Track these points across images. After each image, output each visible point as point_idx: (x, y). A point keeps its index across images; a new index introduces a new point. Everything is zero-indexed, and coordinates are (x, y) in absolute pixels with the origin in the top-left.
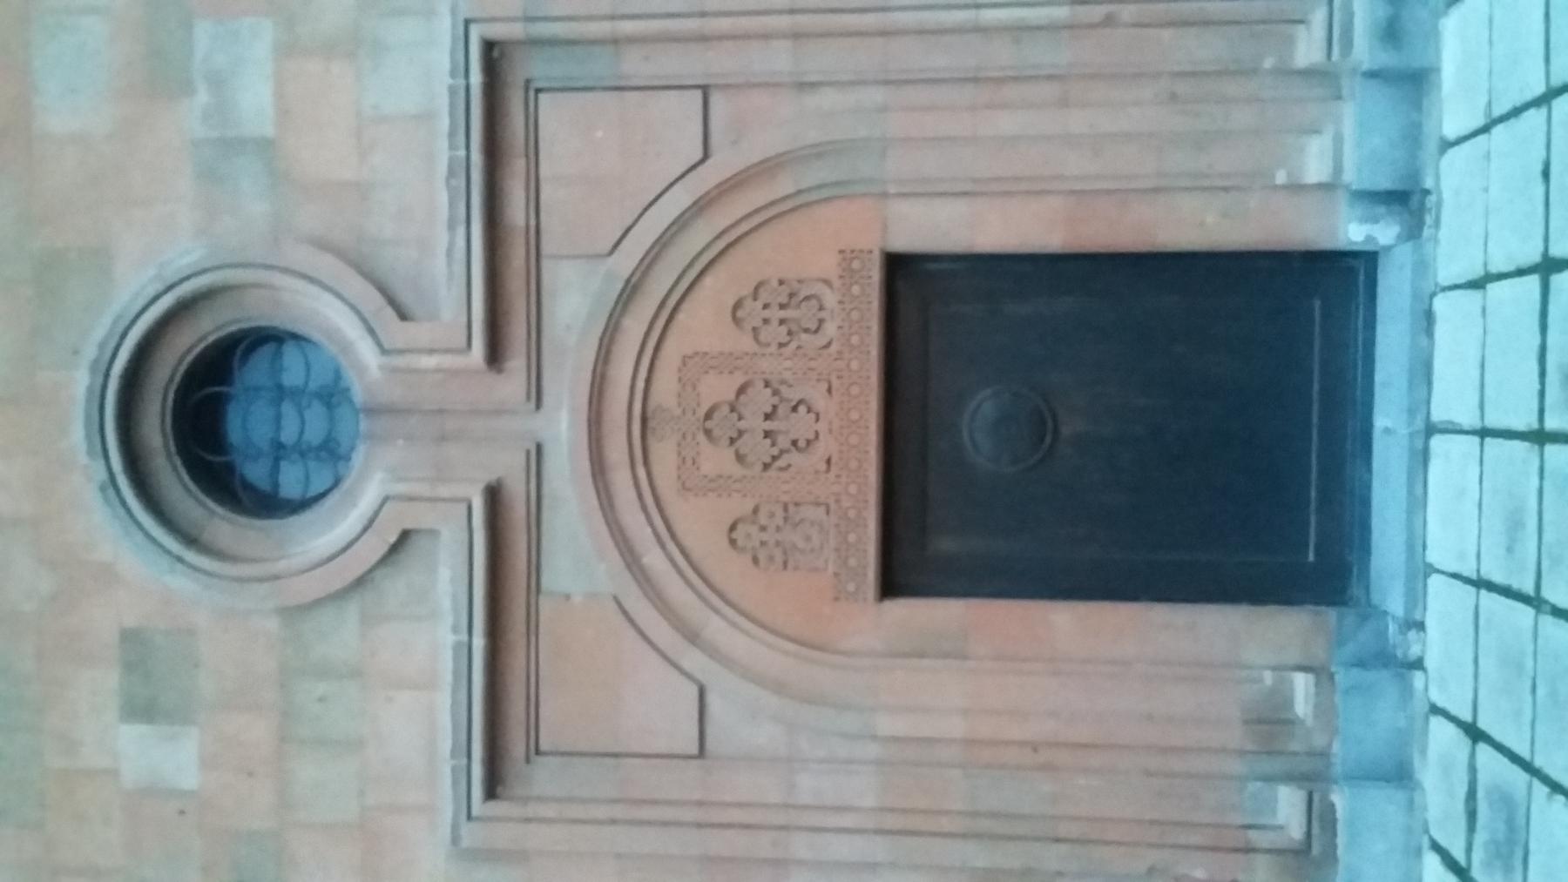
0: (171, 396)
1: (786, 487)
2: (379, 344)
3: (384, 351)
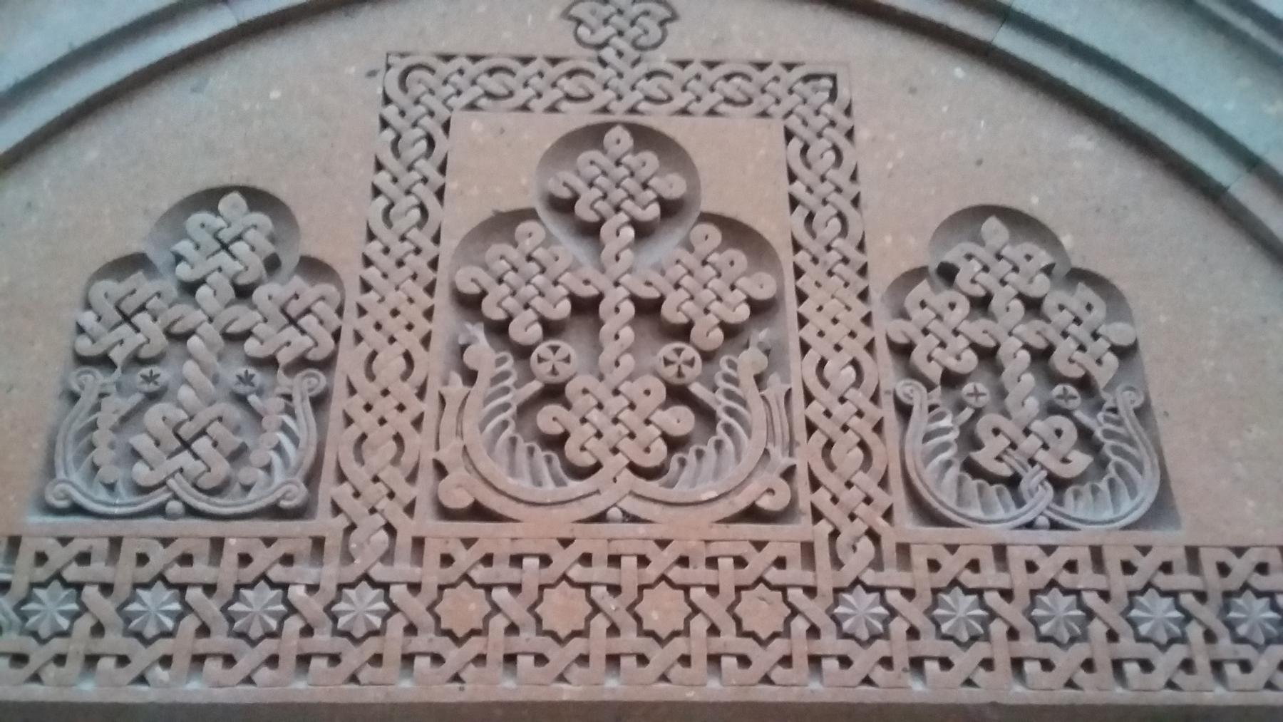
1: (390, 363)
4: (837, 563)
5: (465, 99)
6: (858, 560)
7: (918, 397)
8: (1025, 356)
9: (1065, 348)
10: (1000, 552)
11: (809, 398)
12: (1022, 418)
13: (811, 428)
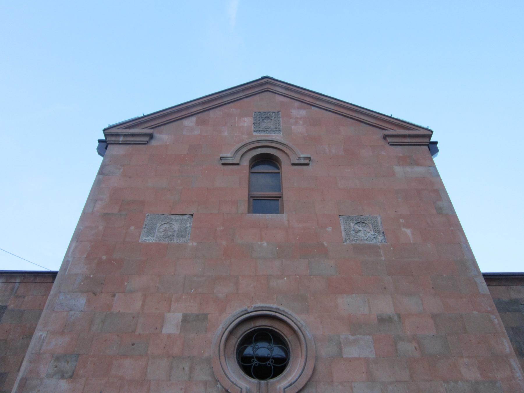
0: (271, 328)
2: (287, 387)
3: (285, 388)
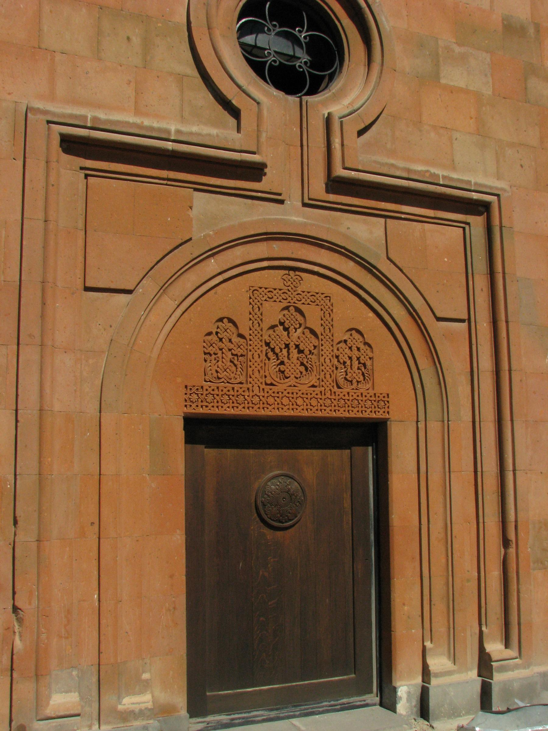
1: (256, 356)
2: (344, 117)
4: (325, 395)
5: (264, 299)
6: (328, 395)
7: (340, 366)
8: (356, 358)
9: (362, 357)
10: (348, 393)
11: (323, 365)
12: (355, 374)
13: (323, 371)
